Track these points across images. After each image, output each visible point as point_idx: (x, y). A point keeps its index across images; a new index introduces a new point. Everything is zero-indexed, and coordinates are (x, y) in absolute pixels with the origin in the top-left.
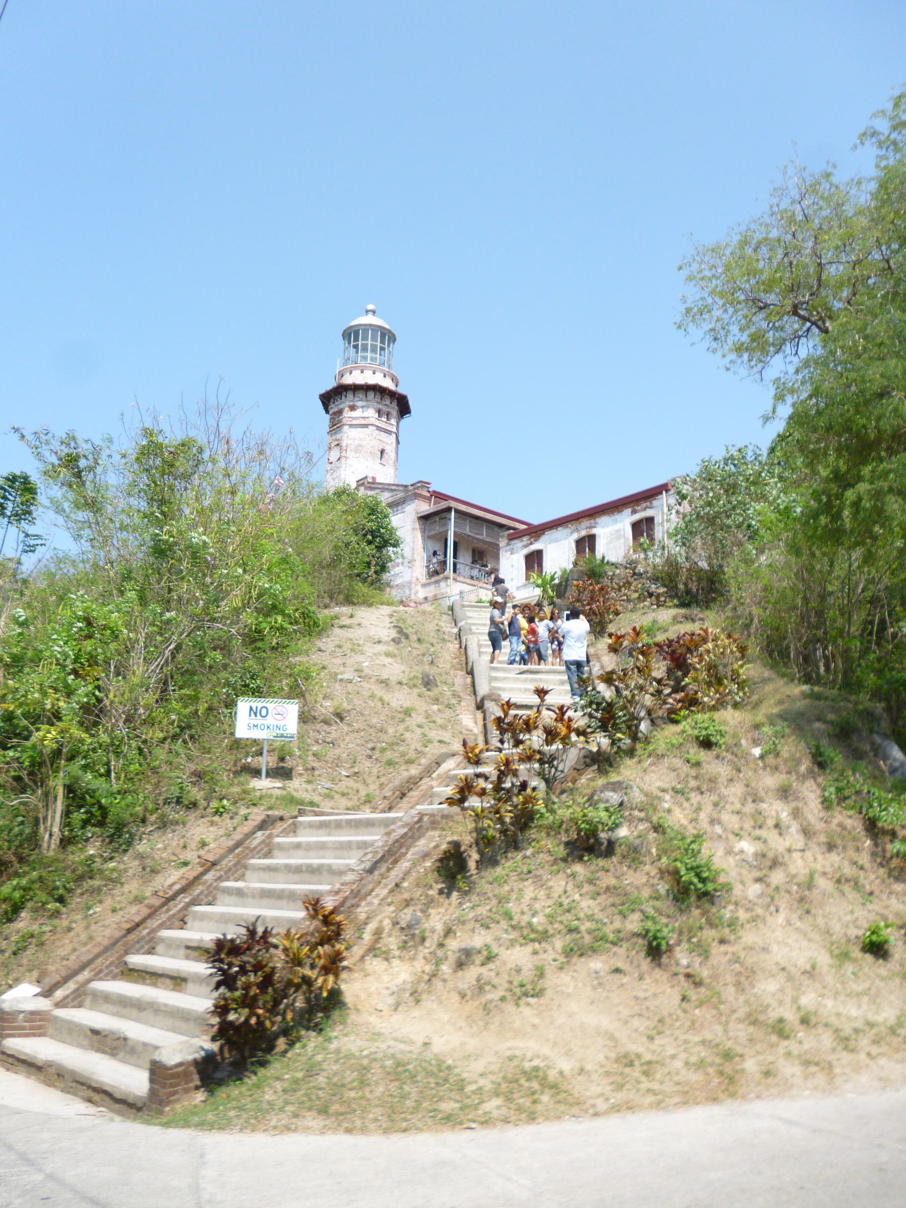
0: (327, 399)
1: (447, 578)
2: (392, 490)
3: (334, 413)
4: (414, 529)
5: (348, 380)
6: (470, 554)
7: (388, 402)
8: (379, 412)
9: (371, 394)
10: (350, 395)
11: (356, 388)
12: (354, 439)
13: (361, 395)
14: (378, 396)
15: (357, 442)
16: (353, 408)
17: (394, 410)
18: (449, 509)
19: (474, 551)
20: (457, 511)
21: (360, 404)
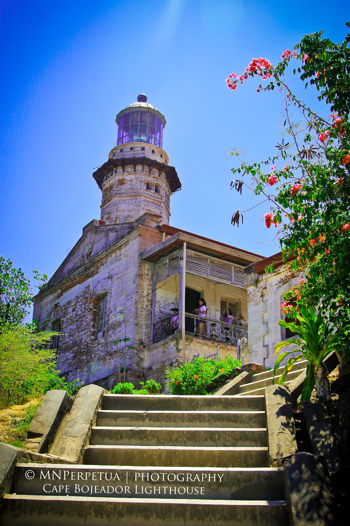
0: (100, 176)
1: (177, 340)
2: (116, 231)
3: (107, 189)
4: (140, 276)
5: (119, 156)
6: (219, 307)
7: (157, 174)
8: (148, 187)
9: (139, 168)
10: (120, 169)
11: (124, 163)
12: (123, 210)
13: (129, 169)
14: (146, 168)
15: (126, 214)
16: (121, 182)
17: (164, 185)
18: (179, 245)
19: (223, 303)
20: (190, 247)
21: (128, 177)
